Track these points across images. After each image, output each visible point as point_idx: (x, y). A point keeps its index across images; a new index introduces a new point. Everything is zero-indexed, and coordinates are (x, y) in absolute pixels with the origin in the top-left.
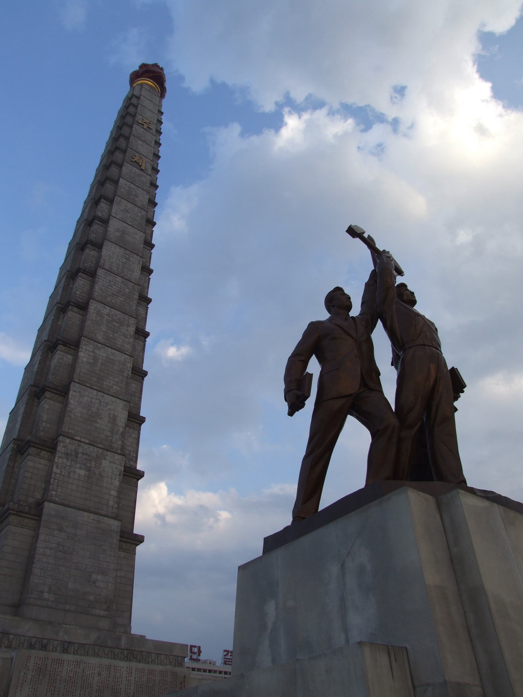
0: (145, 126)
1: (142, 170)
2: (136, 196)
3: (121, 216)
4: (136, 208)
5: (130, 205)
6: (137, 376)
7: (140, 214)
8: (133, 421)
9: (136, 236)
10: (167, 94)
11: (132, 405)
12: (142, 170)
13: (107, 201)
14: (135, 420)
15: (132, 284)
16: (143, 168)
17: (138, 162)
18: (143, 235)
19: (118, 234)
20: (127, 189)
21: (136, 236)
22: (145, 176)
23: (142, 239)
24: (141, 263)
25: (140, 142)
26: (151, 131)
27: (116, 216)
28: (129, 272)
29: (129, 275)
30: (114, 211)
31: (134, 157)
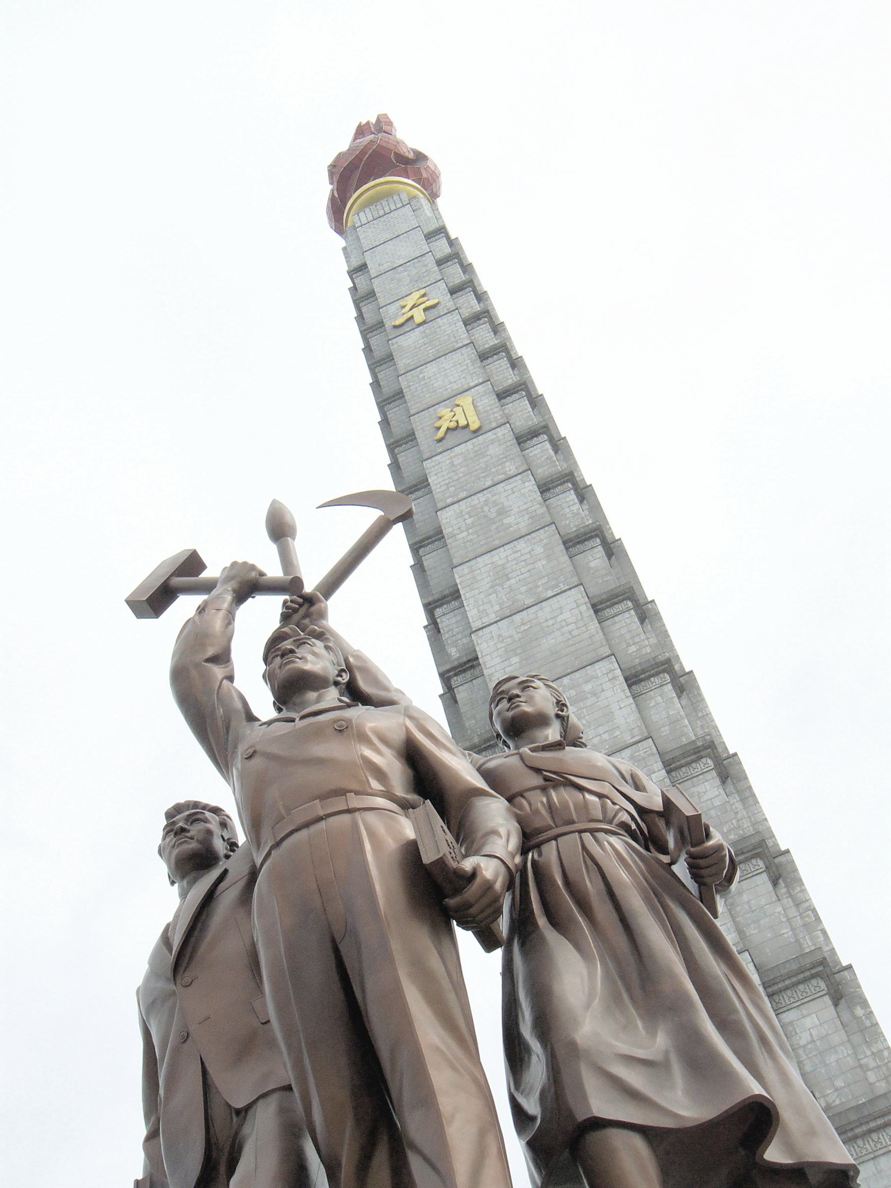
0: (419, 315)
1: (477, 432)
2: (503, 512)
3: (497, 608)
4: (521, 545)
5: (499, 557)
6: (801, 987)
7: (539, 550)
8: (871, 1131)
9: (566, 615)
10: (439, 157)
11: (839, 1083)
12: (477, 432)
13: (448, 603)
14: (872, 1125)
15: (627, 753)
16: (474, 426)
17: (453, 425)
18: (577, 595)
19: (515, 660)
20: (469, 521)
21: (566, 615)
22: (492, 442)
23: (583, 608)
24: (618, 672)
25: (430, 370)
26: (441, 310)
27: (486, 621)
28: (601, 730)
29: (606, 736)
30: (472, 613)
31: (437, 424)
